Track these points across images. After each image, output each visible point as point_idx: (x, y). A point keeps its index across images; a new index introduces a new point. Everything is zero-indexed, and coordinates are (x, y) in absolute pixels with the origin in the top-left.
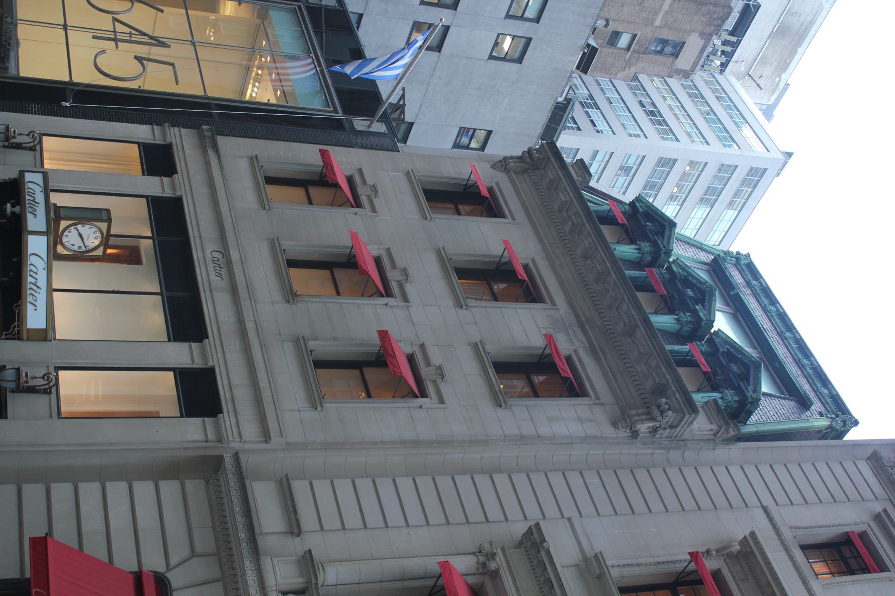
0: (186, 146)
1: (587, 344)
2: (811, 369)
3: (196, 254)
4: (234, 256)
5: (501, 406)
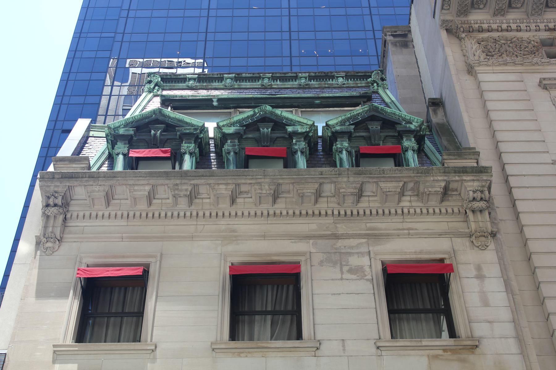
1: (364, 240)
5: (477, 346)
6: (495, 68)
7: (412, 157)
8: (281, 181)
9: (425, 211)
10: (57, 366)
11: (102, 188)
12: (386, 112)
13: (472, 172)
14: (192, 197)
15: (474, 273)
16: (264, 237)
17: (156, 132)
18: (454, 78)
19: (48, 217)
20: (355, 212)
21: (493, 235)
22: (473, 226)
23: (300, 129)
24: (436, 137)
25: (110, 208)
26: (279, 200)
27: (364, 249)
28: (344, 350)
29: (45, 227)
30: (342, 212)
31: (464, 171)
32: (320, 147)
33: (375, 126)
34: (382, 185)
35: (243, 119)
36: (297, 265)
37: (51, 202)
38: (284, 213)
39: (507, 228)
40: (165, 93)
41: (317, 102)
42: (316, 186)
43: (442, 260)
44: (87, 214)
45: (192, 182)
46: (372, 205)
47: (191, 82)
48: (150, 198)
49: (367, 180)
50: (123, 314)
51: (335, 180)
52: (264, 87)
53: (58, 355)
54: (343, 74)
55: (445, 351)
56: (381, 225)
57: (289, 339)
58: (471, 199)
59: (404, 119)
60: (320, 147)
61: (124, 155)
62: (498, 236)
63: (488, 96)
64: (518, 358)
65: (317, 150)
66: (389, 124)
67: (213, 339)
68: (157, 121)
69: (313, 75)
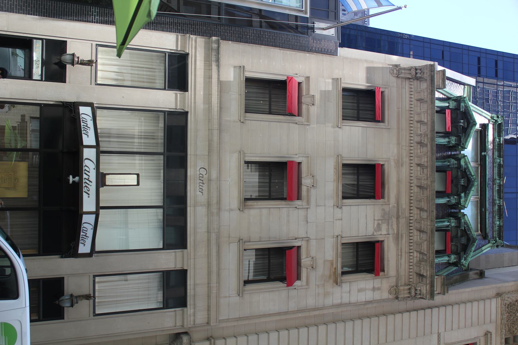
0: (198, 58)
1: (396, 232)
2: (498, 206)
3: (190, 172)
4: (214, 175)
6: (499, 308)
7: (445, 259)
8: (428, 190)
9: (411, 264)
10: (331, 81)
11: (426, 97)
12: (472, 247)
13: (431, 290)
14: (421, 144)
15: (376, 286)
16: (399, 181)
17: (462, 123)
18: (494, 286)
19: (410, 70)
20: (411, 228)
21: (397, 298)
22: (402, 288)
23: (462, 200)
24: (460, 273)
25: (415, 101)
26: (419, 189)
27: (391, 232)
28: (337, 220)
29: (404, 69)
30: (411, 221)
31: (432, 286)
32: (453, 211)
33: (464, 241)
34: (425, 243)
35: (469, 170)
36: (382, 197)
37: (418, 71)
38: (412, 191)
39: (402, 305)
40: (491, 127)
41: (483, 210)
42: (425, 208)
43: (384, 271)
44: (412, 90)
45: (429, 144)
46: (415, 237)
47: (498, 140)
48: (420, 122)
49: (428, 235)
50: (358, 110)
51: (429, 218)
52: (494, 180)
53: (336, 81)
54: (501, 224)
55: (335, 269)
56: (404, 242)
57: (343, 192)
58: (417, 288)
59: (467, 256)
60: (453, 211)
61: (448, 106)
62: (397, 300)
63: (482, 303)
64: (331, 303)
65: (451, 209)
66: (465, 248)
67: (343, 155)
68: (469, 123)
69: (502, 208)
